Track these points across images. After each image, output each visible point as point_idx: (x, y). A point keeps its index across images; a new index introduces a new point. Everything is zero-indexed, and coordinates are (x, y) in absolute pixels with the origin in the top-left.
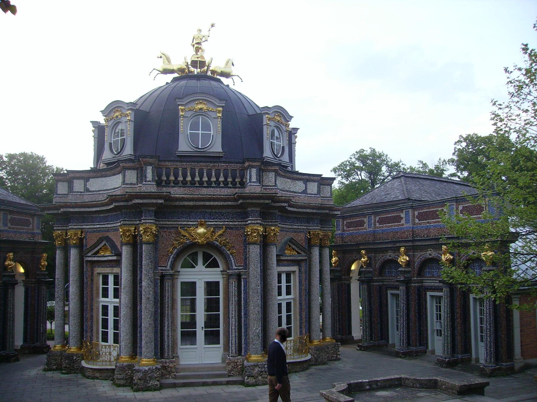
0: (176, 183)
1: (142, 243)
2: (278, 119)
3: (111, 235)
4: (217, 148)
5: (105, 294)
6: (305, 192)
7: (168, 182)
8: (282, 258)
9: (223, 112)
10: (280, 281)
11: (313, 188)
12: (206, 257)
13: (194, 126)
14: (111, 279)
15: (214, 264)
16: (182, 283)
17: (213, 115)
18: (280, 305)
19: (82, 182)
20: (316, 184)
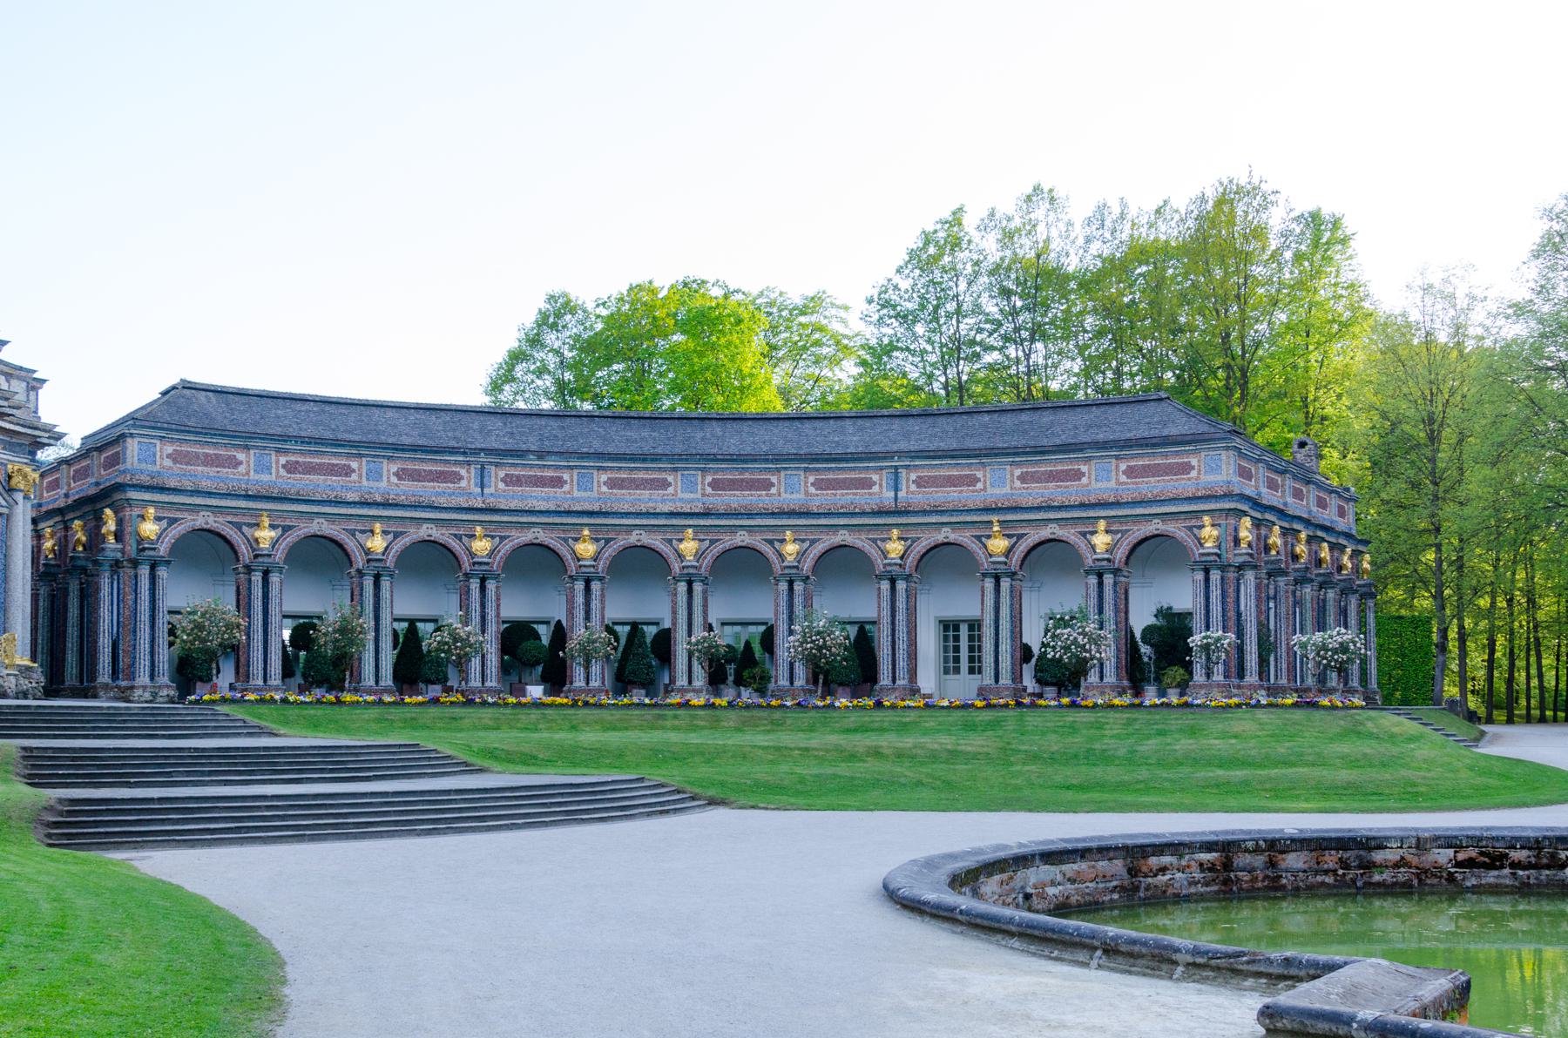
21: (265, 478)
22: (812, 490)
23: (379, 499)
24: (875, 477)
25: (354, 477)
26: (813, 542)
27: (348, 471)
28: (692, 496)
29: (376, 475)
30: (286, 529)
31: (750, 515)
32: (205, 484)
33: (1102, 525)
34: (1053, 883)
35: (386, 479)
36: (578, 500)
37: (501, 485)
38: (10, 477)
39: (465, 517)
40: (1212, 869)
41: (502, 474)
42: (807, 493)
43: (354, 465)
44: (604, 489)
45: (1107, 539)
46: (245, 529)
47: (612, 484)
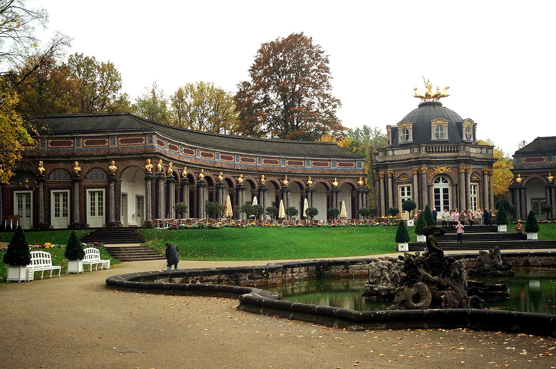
0: (433, 151)
2: (468, 123)
3: (406, 172)
4: (446, 137)
5: (403, 194)
6: (481, 153)
7: (430, 152)
8: (472, 179)
9: (448, 124)
11: (484, 150)
12: (443, 179)
13: (437, 130)
14: (406, 189)
15: (446, 182)
16: (434, 189)
17: (444, 125)
18: (471, 198)
20: (486, 149)
38: (483, 172)
46: (546, 177)
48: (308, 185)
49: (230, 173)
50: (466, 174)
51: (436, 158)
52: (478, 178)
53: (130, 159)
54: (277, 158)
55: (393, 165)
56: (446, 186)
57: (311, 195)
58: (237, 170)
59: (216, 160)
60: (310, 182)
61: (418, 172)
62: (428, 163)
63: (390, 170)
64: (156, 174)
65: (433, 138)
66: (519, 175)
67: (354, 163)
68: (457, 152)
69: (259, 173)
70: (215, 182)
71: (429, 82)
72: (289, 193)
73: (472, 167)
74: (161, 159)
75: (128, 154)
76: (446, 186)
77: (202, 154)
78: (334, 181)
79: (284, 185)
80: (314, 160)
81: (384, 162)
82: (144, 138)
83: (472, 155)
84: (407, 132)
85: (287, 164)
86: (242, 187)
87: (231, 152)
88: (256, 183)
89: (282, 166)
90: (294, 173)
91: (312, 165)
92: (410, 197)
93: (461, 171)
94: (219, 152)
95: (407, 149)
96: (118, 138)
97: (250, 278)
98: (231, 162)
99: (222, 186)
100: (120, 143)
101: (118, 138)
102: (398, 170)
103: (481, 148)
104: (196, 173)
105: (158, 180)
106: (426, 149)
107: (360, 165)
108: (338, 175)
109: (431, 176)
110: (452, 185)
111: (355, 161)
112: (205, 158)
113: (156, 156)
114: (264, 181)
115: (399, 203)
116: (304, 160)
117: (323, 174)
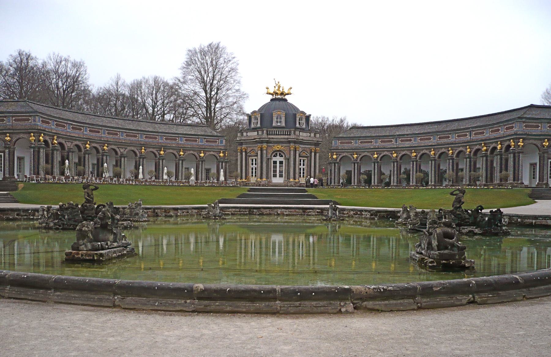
1: (263, 150)
4: (284, 125)
6: (310, 136)
7: (270, 134)
10: (300, 161)
13: (277, 118)
14: (254, 160)
15: (282, 156)
16: (273, 161)
17: (282, 115)
19: (245, 133)
21: (356, 145)
22: (457, 138)
23: (377, 147)
24: (467, 134)
25: (373, 143)
26: (456, 150)
27: (372, 142)
28: (435, 141)
29: (376, 142)
30: (360, 154)
31: (443, 145)
32: (346, 148)
33: (499, 142)
34: (286, 212)
35: (379, 143)
36: (414, 144)
37: (400, 142)
38: (311, 150)
39: (392, 149)
40: (319, 212)
41: (400, 140)
42: (456, 139)
43: (373, 141)
44: (419, 141)
45: (500, 146)
47: (421, 140)
48: (180, 155)
49: (115, 145)
50: (295, 151)
51: (273, 139)
52: (307, 154)
53: (21, 133)
54: (156, 135)
55: (246, 143)
56: (282, 159)
57: (182, 163)
58: (121, 143)
59: (103, 135)
60: (181, 153)
61: (261, 148)
62: (267, 142)
63: (244, 146)
64: (38, 144)
65: (274, 125)
66: (335, 153)
67: (218, 141)
68: (290, 135)
69: (141, 145)
70: (101, 151)
71: (279, 83)
72: (164, 161)
73: (302, 146)
74: (42, 133)
75: (19, 130)
76: (282, 159)
77: (90, 131)
78: (201, 153)
79: (161, 155)
80: (186, 137)
81: (240, 140)
82: (30, 118)
83: (301, 138)
84: (257, 120)
85: (165, 140)
86: (125, 155)
87: (116, 130)
88: (138, 152)
89: (160, 141)
90: (169, 147)
91: (185, 141)
92: (256, 166)
93: (291, 149)
94: (105, 129)
95: (255, 131)
96: (12, 118)
97: (17, 215)
98: (116, 137)
99: (105, 154)
100: (14, 122)
101: (12, 118)
102: (250, 147)
103: (310, 133)
104: (84, 144)
105: (39, 148)
106: (267, 131)
107: (222, 142)
108: (204, 148)
109: (270, 151)
110: (285, 159)
111: (218, 139)
112: (92, 134)
113: (38, 132)
114: (144, 151)
115: (249, 170)
116: (178, 137)
117: (193, 148)
